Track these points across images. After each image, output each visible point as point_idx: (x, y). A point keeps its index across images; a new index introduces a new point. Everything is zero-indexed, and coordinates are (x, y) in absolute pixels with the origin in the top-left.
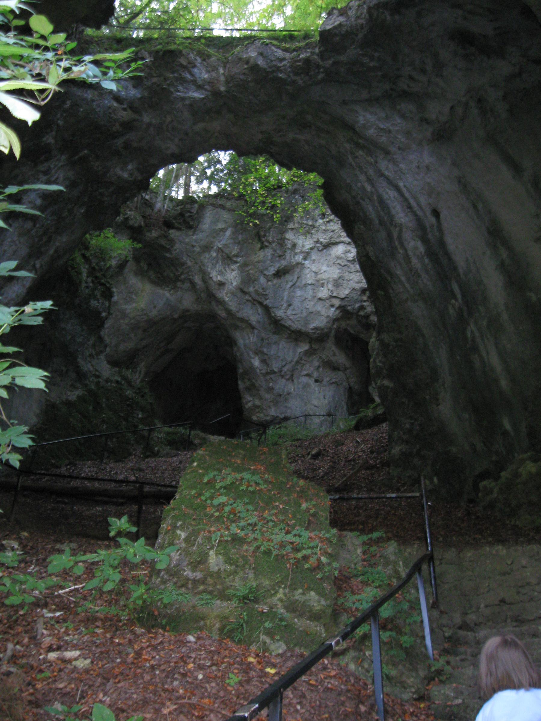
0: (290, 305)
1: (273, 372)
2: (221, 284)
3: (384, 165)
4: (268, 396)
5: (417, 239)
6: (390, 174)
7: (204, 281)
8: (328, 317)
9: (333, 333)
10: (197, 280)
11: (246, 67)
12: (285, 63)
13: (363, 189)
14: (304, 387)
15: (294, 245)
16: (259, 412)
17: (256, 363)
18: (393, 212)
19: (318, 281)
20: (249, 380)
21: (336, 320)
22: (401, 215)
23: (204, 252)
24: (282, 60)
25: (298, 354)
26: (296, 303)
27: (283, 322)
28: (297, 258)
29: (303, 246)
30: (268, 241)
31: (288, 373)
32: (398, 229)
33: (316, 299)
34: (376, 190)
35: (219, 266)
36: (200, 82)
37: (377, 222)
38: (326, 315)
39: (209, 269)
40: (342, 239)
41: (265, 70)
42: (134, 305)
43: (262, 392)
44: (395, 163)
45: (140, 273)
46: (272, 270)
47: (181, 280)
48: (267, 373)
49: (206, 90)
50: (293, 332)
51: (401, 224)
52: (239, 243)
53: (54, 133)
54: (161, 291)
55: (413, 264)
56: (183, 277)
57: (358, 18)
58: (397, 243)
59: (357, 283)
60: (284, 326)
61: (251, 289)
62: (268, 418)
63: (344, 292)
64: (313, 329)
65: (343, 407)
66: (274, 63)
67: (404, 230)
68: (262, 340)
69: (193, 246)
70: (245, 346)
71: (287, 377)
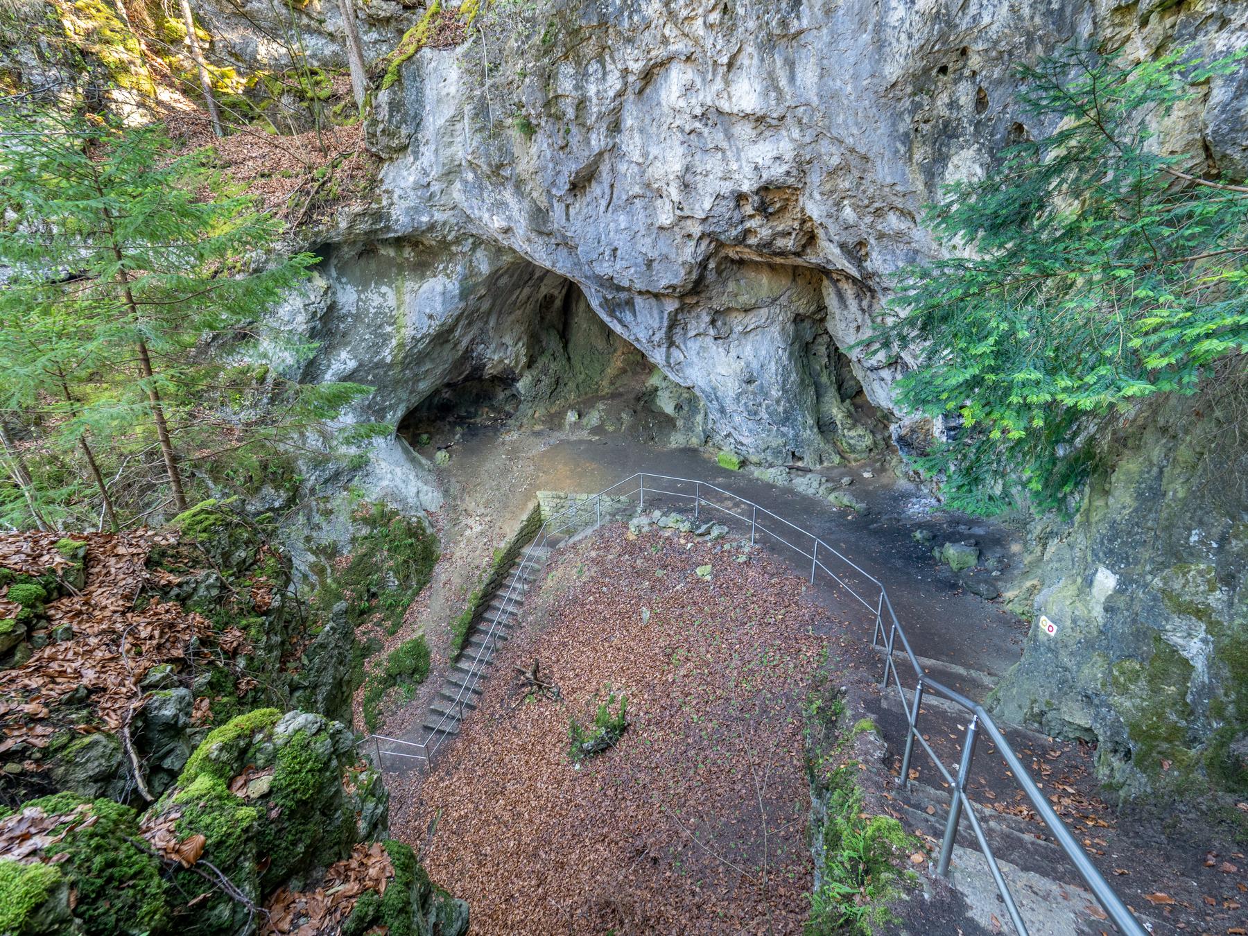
2: (507, 231)
23: (451, 183)
25: (666, 316)
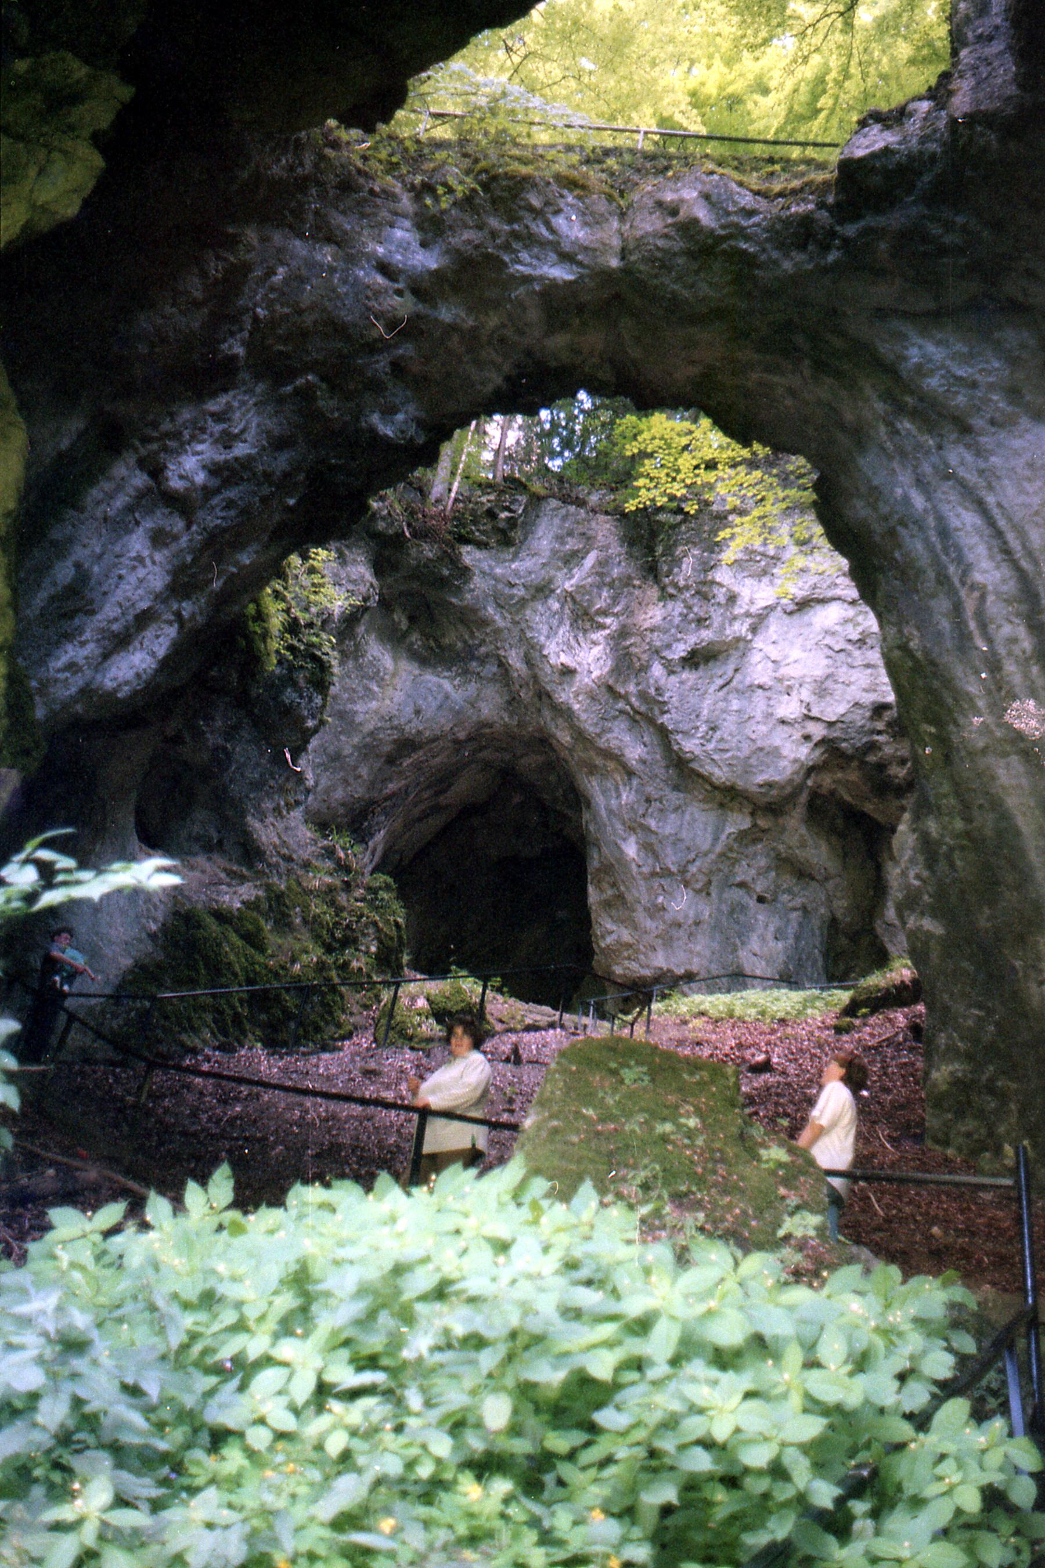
0: (714, 729)
1: (666, 873)
2: (568, 672)
3: (957, 456)
4: (649, 924)
5: (1017, 621)
6: (968, 476)
7: (528, 661)
8: (796, 761)
9: (804, 798)
10: (515, 659)
11: (670, 221)
12: (756, 219)
13: (906, 499)
14: (732, 912)
15: (732, 598)
16: (629, 958)
17: (631, 849)
18: (971, 557)
19: (780, 680)
20: (614, 885)
21: (811, 770)
22: (985, 564)
23: (534, 598)
24: (750, 213)
25: (723, 837)
26: (729, 725)
27: (694, 765)
28: (736, 626)
29: (752, 602)
30: (676, 585)
31: (700, 877)
32: (976, 594)
33: (772, 721)
34: (934, 507)
35: (564, 631)
36: (566, 247)
37: (931, 574)
38: (792, 756)
39: (542, 639)
40: (838, 592)
41: (712, 231)
42: (374, 704)
43: (640, 916)
44: (979, 452)
45: (394, 638)
46: (680, 650)
47: (478, 658)
48: (653, 874)
49: (580, 264)
50: (715, 787)
51: (985, 586)
52: (611, 585)
53: (246, 334)
54: (435, 679)
55: (1004, 673)
56: (483, 650)
57: (924, 140)
58: (972, 625)
59: (865, 690)
60: (700, 775)
61: (632, 688)
62: (647, 973)
63: (835, 709)
64: (761, 786)
65: (815, 961)
66: (734, 219)
67: (991, 598)
68: (648, 800)
69: (512, 586)
70: (610, 812)
71: (698, 886)
